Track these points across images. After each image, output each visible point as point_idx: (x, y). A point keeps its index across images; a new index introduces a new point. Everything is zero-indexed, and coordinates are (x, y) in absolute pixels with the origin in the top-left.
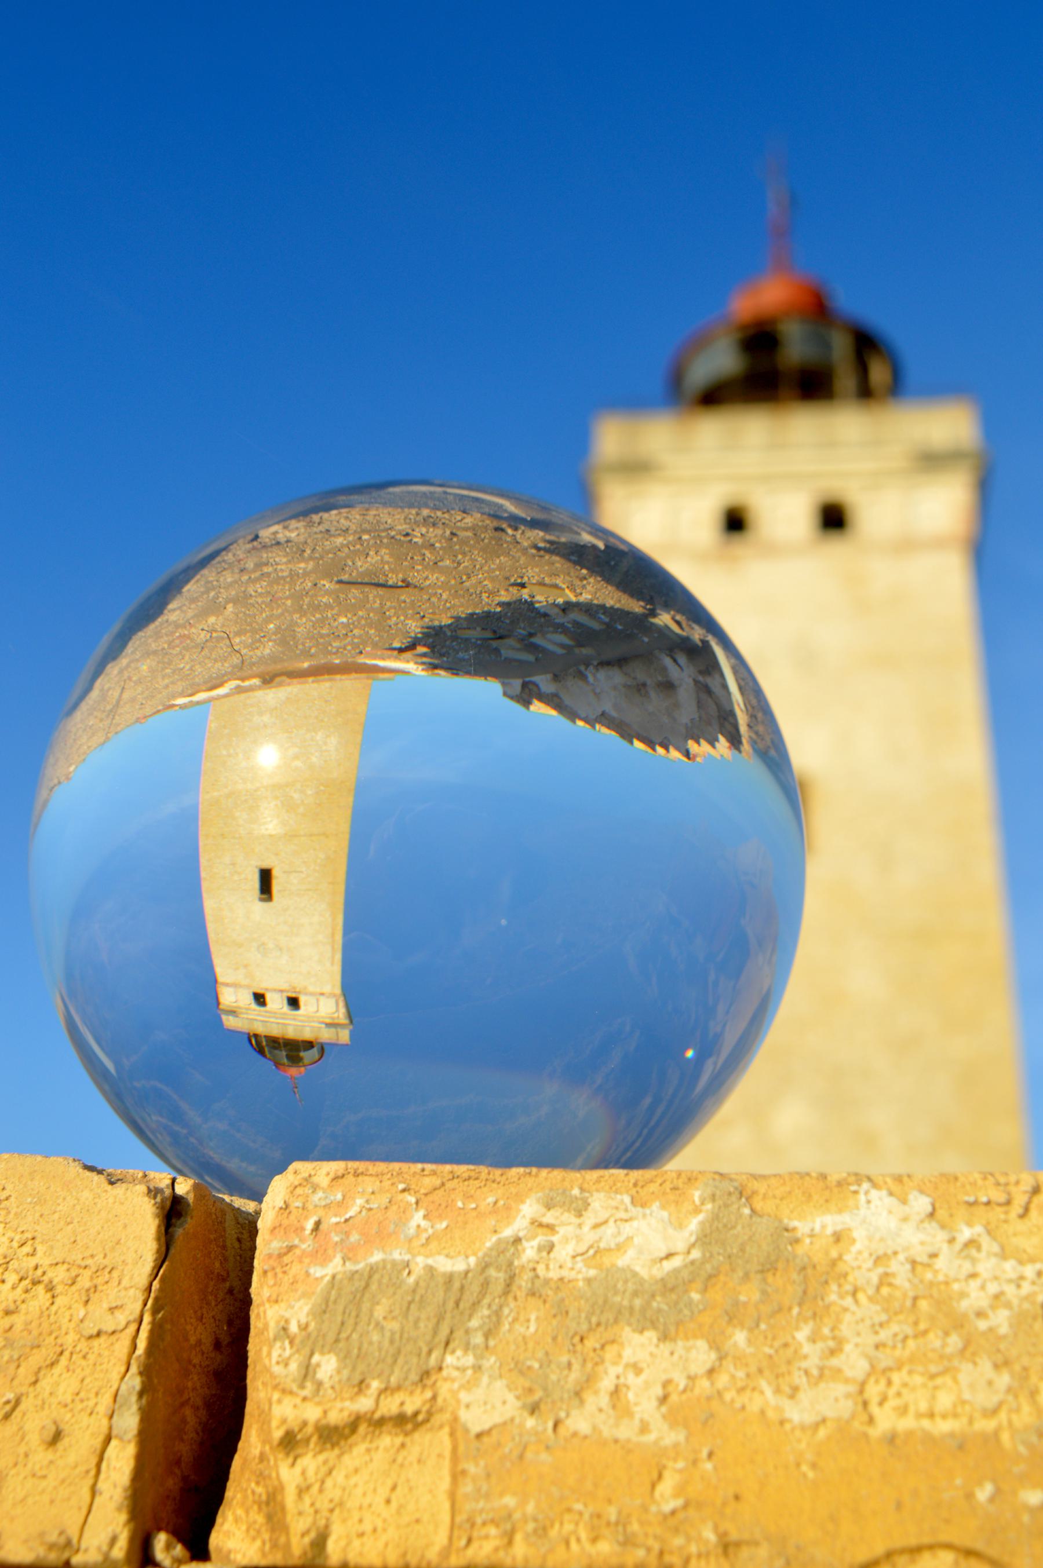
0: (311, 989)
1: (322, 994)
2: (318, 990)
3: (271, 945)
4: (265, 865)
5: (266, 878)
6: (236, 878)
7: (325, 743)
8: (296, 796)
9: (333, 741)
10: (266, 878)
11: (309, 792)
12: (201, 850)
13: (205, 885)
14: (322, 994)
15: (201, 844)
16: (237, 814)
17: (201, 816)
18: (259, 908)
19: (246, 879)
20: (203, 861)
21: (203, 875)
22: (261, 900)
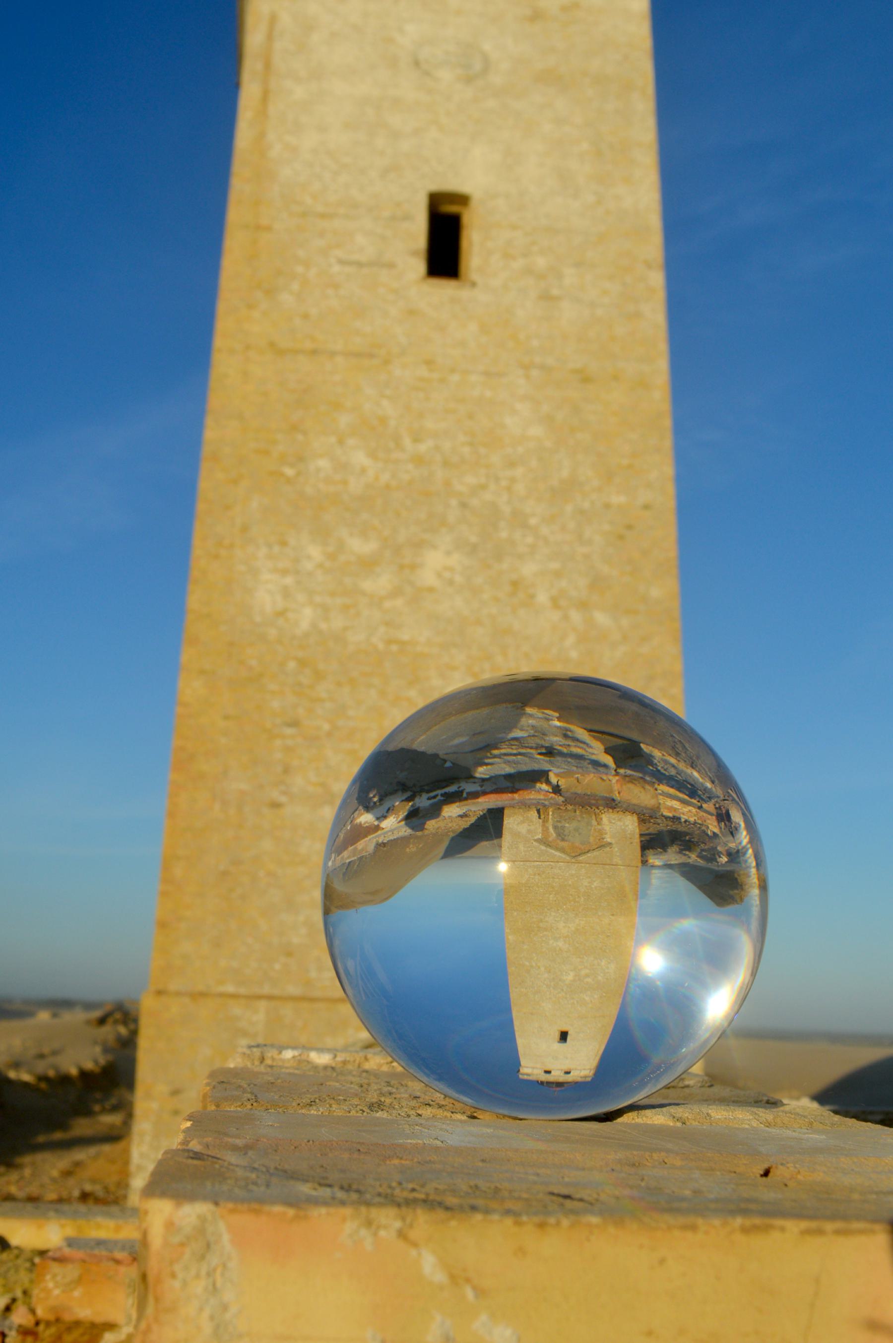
3: (446, 75)
4: (444, 288)
5: (444, 250)
6: (541, 262)
7: (286, 593)
8: (360, 458)
9: (266, 595)
10: (444, 250)
12: (663, 347)
13: (652, 246)
15: (662, 365)
16: (536, 431)
17: (668, 443)
18: (472, 176)
20: (654, 315)
21: (657, 279)
22: (462, 199)
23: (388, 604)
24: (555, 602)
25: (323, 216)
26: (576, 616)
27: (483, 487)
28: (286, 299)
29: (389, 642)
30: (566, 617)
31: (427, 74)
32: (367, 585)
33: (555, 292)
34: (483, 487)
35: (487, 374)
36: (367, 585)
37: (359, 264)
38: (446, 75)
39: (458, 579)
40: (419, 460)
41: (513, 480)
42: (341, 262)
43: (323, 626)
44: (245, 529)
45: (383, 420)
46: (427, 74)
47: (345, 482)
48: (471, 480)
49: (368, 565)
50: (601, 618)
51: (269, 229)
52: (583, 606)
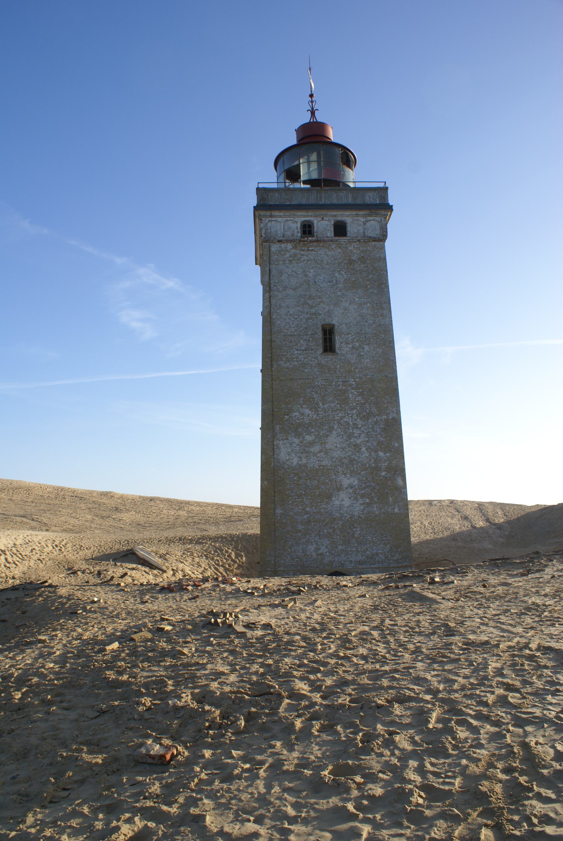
1: (279, 241)
8: (307, 411)
14: (279, 241)
19: (349, 344)
23: (318, 455)
25: (291, 335)
27: (345, 417)
32: (312, 450)
33: (362, 354)
36: (312, 450)
42: (297, 350)
43: (300, 463)
47: (303, 419)
49: (312, 444)
50: (381, 454)
52: (376, 451)
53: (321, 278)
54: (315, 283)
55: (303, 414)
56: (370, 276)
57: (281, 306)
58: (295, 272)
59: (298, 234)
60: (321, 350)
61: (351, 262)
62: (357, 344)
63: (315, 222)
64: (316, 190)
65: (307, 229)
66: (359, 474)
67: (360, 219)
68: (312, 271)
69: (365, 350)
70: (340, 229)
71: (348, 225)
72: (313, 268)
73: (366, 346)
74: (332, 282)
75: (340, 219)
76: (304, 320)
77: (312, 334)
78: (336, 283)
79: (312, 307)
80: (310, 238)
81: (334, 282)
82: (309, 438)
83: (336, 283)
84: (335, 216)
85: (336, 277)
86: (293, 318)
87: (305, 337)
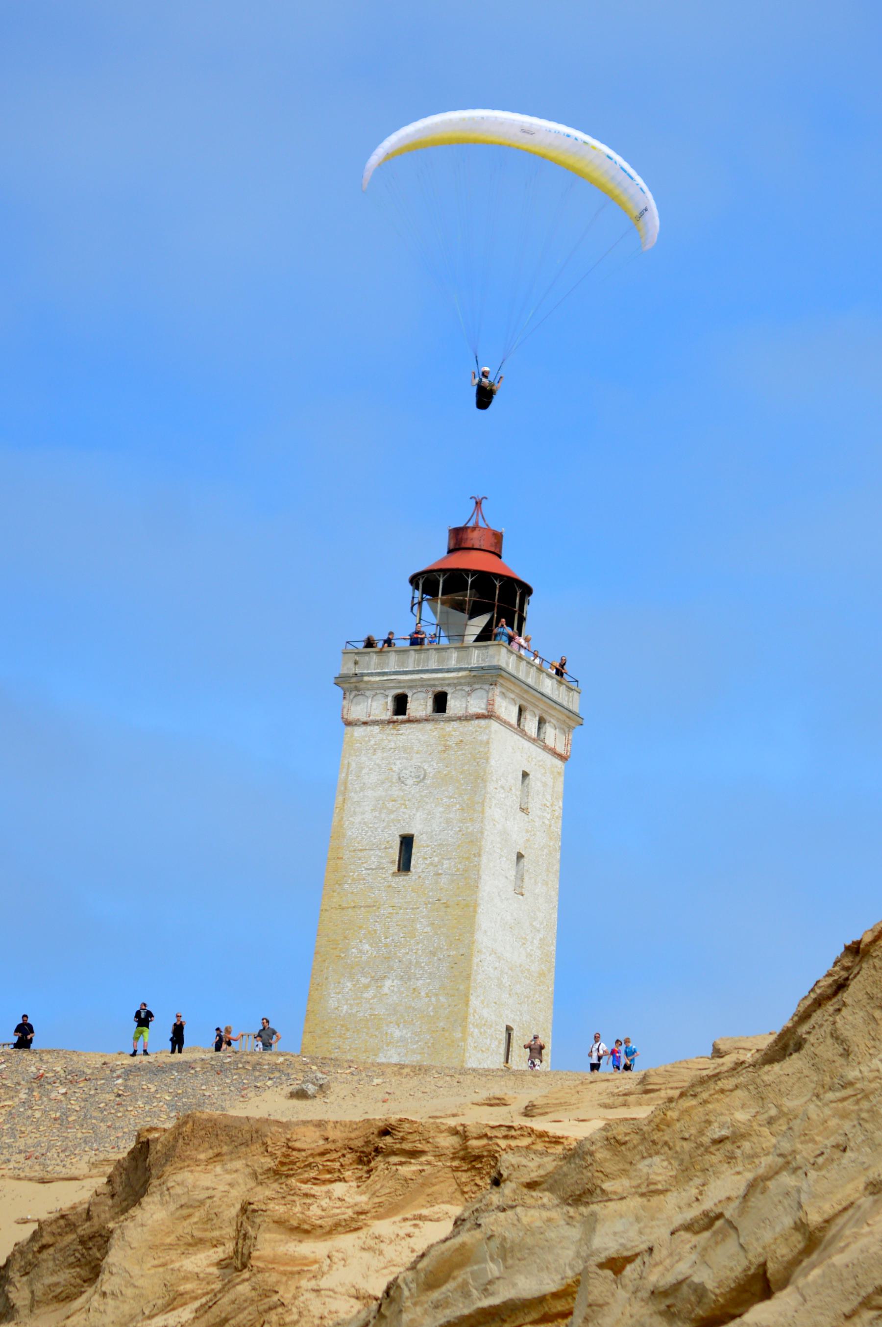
0: (376, 729)
1: (365, 723)
2: (369, 728)
8: (367, 947)
11: (353, 950)
14: (365, 723)
16: (428, 929)
24: (427, 995)
26: (433, 999)
27: (408, 953)
28: (346, 886)
29: (371, 1015)
30: (430, 1000)
31: (403, 782)
32: (365, 995)
33: (440, 871)
34: (408, 953)
35: (412, 909)
36: (365, 995)
37: (373, 869)
38: (410, 782)
39: (396, 989)
40: (386, 946)
41: (418, 949)
44: (327, 979)
45: (375, 931)
46: (403, 782)
48: (403, 951)
50: (442, 999)
51: (342, 858)
53: (407, 772)
54: (399, 778)
55: (361, 951)
56: (466, 768)
57: (355, 813)
58: (378, 765)
59: (388, 715)
60: (395, 868)
61: (447, 748)
62: (436, 859)
63: (410, 695)
64: (415, 650)
65: (401, 704)
66: (414, 1024)
67: (464, 688)
68: (398, 762)
69: (445, 866)
70: (440, 702)
71: (449, 697)
72: (399, 759)
73: (445, 862)
74: (419, 777)
75: (439, 689)
76: (379, 830)
77: (386, 848)
78: (424, 778)
79: (392, 812)
80: (400, 717)
81: (422, 777)
82: (364, 981)
83: (424, 778)
84: (434, 685)
85: (425, 770)
86: (368, 827)
87: (378, 852)
